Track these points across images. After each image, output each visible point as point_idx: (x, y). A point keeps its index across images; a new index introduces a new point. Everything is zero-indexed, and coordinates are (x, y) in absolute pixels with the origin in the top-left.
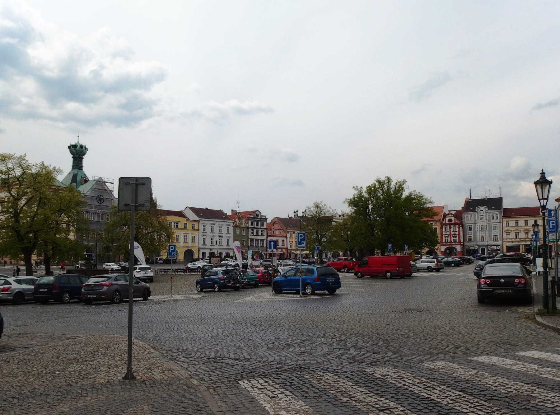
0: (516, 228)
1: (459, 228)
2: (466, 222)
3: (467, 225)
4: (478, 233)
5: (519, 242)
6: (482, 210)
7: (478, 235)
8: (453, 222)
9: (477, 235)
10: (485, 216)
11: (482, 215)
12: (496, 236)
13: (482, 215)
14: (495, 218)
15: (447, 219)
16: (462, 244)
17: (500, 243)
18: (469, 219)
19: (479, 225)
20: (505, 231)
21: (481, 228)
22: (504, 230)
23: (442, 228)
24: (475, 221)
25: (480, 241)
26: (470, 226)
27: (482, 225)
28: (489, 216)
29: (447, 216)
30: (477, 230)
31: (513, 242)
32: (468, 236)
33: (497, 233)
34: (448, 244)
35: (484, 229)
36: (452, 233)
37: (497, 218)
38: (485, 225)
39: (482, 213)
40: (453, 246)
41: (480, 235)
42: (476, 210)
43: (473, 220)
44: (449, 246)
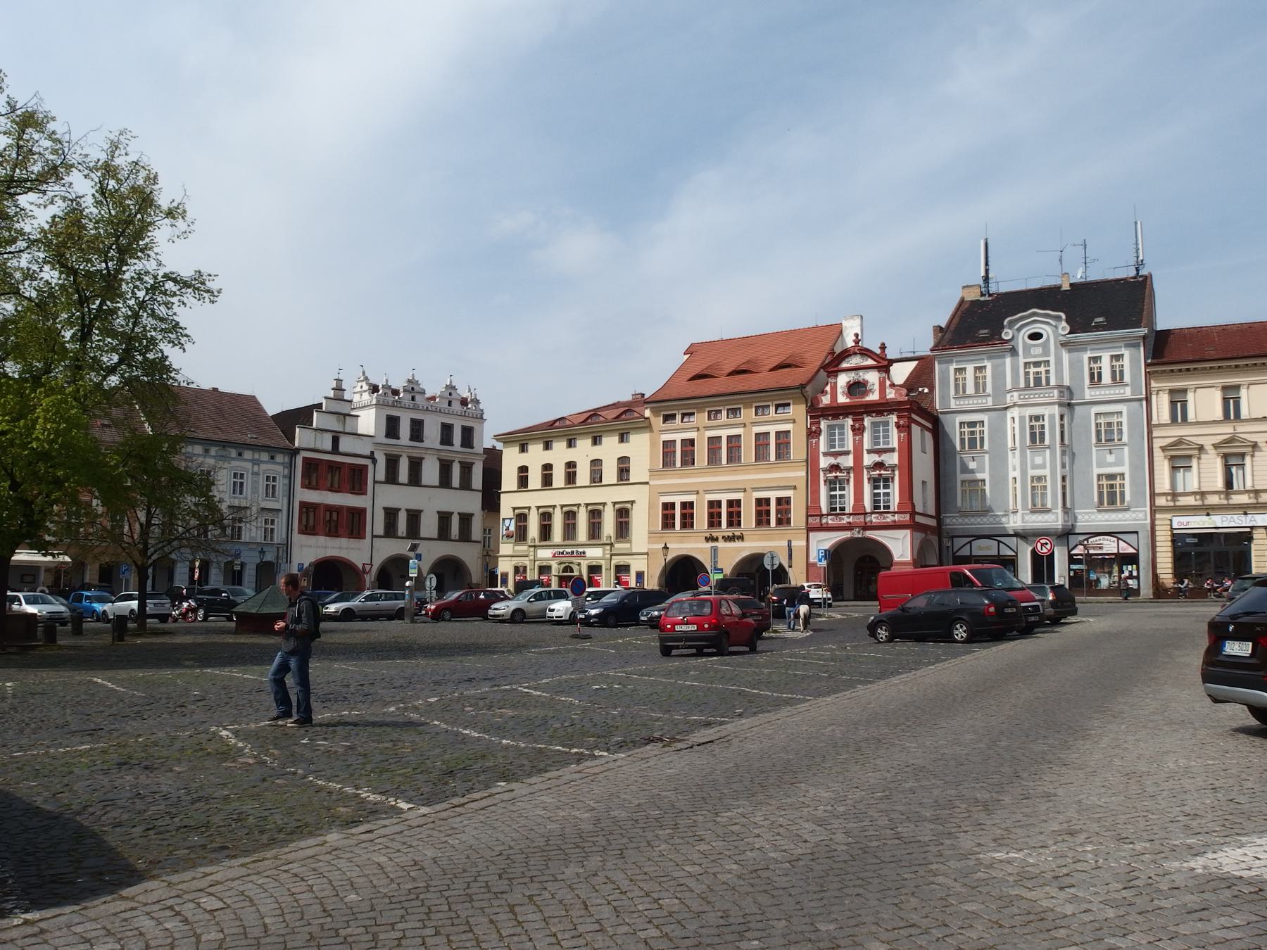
0: (1227, 429)
1: (904, 428)
2: (954, 405)
3: (960, 418)
4: (1014, 460)
5: (1244, 509)
6: (1035, 336)
7: (1017, 474)
8: (874, 397)
9: (1012, 474)
10: (1052, 368)
11: (1037, 364)
12: (1111, 477)
13: (1037, 364)
14: (1106, 378)
15: (843, 380)
16: (933, 522)
17: (1137, 517)
18: (970, 390)
19: (1022, 418)
20: (1163, 449)
21: (1033, 435)
22: (1157, 444)
23: (813, 434)
24: (1000, 390)
25: (1024, 506)
26: (972, 424)
27: (1037, 418)
28: (1075, 367)
29: (844, 365)
30: (1010, 444)
31: (1208, 510)
32: (963, 482)
33: (1121, 462)
34: (846, 520)
35: (1047, 442)
36: (868, 460)
37: (1117, 377)
38: (1052, 417)
39: (1039, 350)
40: (869, 534)
41: (1024, 472)
42: (1007, 334)
43: (989, 390)
44: (847, 535)
